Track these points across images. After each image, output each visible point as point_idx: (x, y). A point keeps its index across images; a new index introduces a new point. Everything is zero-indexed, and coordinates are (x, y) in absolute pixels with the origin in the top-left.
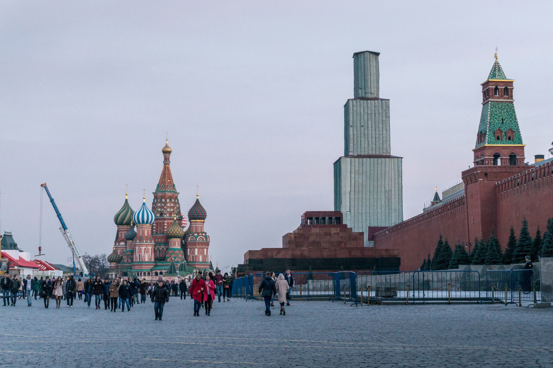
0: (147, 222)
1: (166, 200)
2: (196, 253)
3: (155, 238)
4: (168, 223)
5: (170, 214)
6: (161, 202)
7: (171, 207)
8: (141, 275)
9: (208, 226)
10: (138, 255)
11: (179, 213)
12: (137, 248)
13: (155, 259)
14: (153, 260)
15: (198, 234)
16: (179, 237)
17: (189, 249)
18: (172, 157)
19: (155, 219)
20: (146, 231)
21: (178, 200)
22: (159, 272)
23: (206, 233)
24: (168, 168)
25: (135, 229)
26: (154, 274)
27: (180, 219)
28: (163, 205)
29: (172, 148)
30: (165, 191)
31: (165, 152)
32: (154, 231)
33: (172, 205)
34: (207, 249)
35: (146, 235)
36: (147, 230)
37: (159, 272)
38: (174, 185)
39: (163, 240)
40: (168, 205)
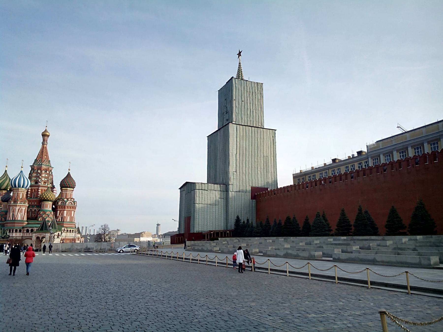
0: (23, 187)
1: (41, 172)
2: (65, 215)
3: (29, 201)
4: (42, 190)
5: (45, 182)
6: (37, 173)
7: (45, 178)
8: (13, 232)
9: (76, 194)
10: (11, 214)
11: (52, 183)
12: (11, 208)
13: (28, 218)
14: (25, 219)
15: (68, 199)
16: (51, 201)
17: (58, 211)
18: (49, 140)
19: (31, 186)
20: (21, 194)
21: (52, 173)
22: (30, 229)
23: (74, 199)
24: (46, 148)
25: (11, 194)
26: (25, 231)
27: (53, 187)
28: (38, 175)
29: (50, 132)
30: (40, 166)
31: (43, 135)
32: (29, 195)
33: (47, 176)
34: (74, 211)
35: (21, 198)
36: (22, 193)
37: (30, 229)
38: (49, 161)
39: (36, 203)
40: (43, 175)
